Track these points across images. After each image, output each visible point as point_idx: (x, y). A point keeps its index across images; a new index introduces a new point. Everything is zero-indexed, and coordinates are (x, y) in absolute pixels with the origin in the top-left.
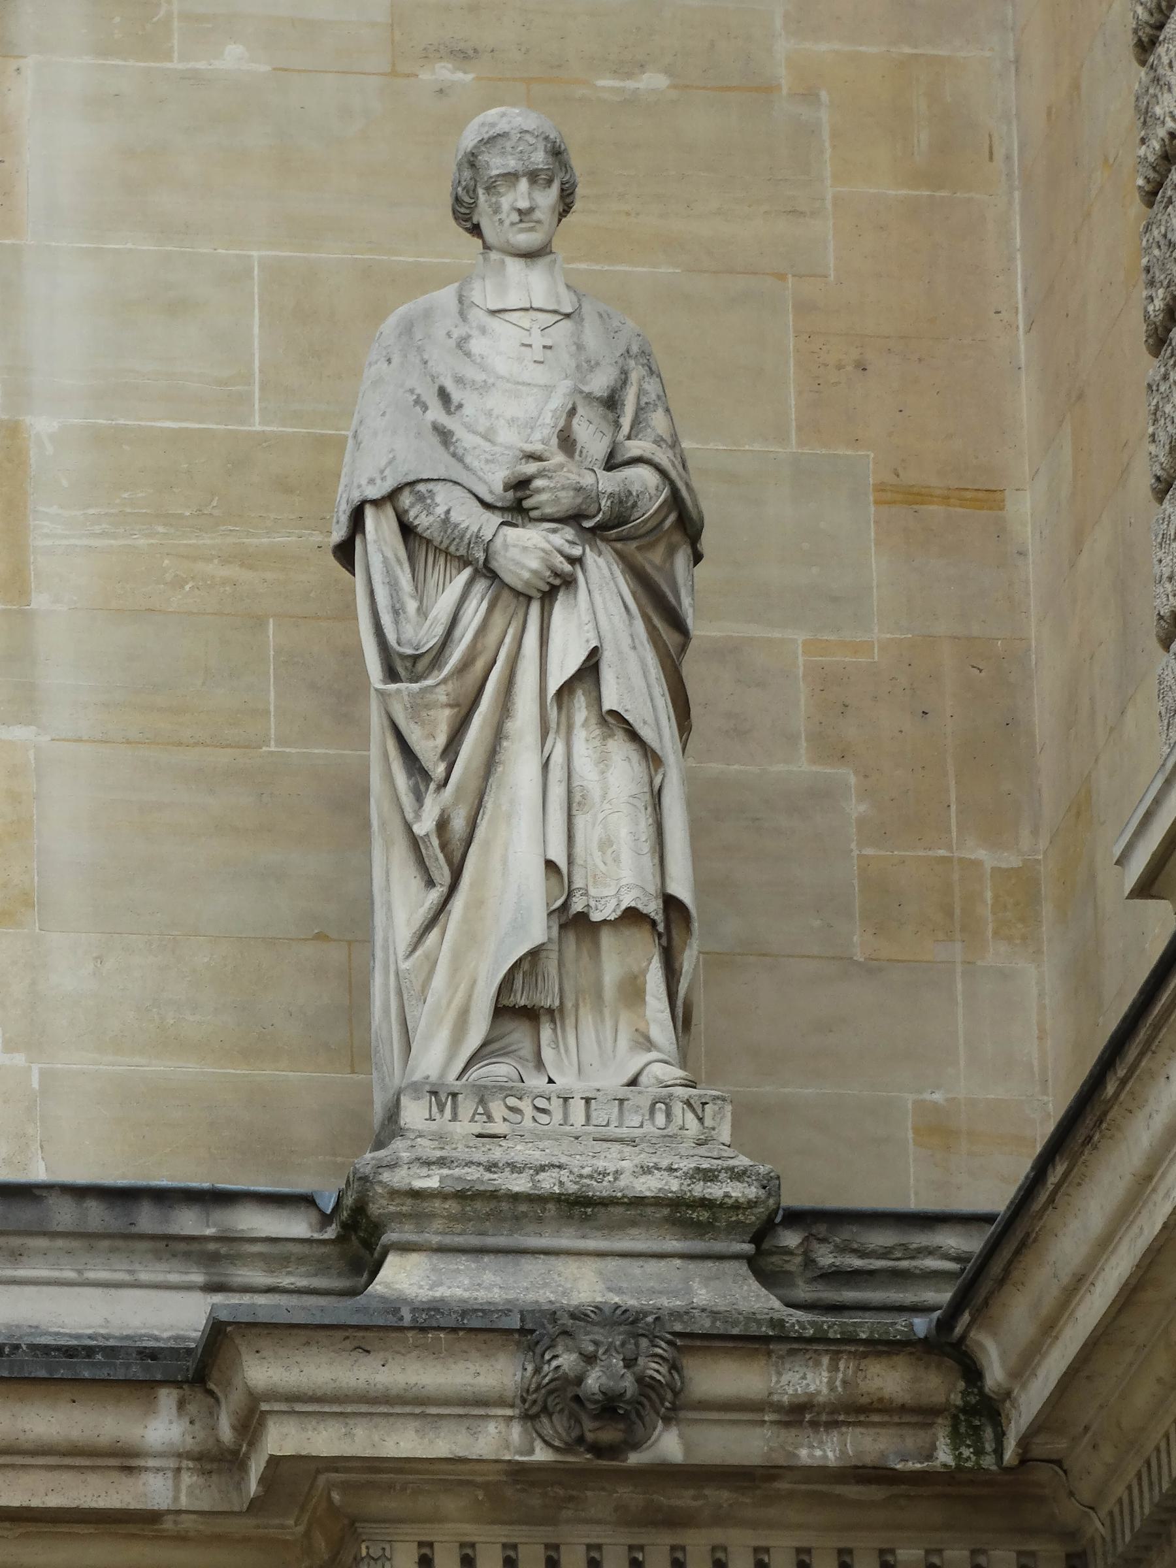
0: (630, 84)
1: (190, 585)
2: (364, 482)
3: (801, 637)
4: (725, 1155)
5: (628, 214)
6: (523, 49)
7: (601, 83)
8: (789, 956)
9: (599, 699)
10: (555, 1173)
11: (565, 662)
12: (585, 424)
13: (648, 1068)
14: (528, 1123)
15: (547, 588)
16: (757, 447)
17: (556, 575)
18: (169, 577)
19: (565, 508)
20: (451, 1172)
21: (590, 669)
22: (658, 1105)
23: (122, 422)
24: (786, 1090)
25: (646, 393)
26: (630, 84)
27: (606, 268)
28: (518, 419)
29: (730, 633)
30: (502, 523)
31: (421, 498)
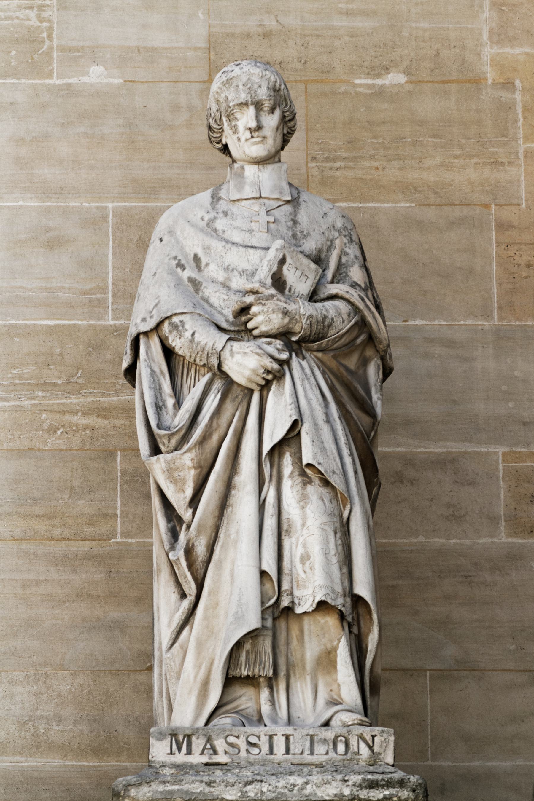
0: (379, 82)
1: (61, 430)
2: (139, 321)
3: (501, 450)
4: (387, 770)
5: (377, 169)
6: (303, 62)
7: (357, 81)
8: (493, 670)
9: (300, 459)
10: (257, 785)
11: (275, 431)
12: (293, 270)
13: (336, 715)
14: (243, 754)
15: (263, 383)
16: (469, 322)
17: (268, 372)
18: (45, 426)
19: (277, 326)
20: (181, 787)
21: (292, 437)
22: (339, 738)
23: (13, 322)
24: (490, 764)
25: (347, 254)
26: (379, 82)
27: (361, 205)
28: (246, 270)
29: (450, 450)
30: (229, 339)
31: (176, 327)
